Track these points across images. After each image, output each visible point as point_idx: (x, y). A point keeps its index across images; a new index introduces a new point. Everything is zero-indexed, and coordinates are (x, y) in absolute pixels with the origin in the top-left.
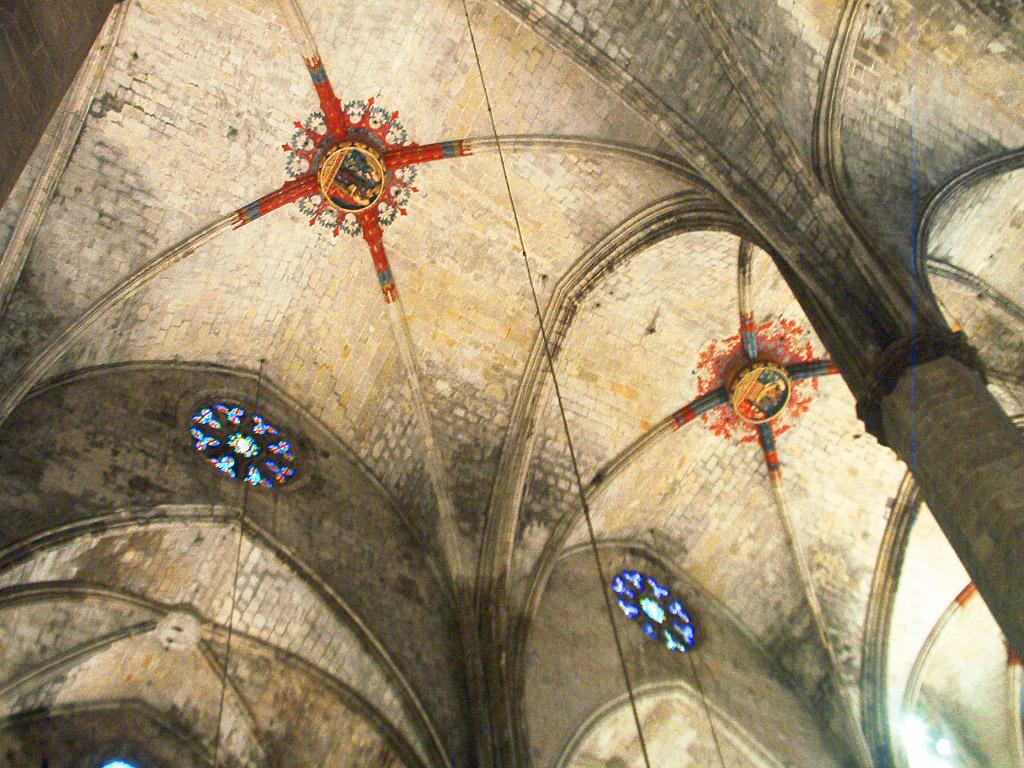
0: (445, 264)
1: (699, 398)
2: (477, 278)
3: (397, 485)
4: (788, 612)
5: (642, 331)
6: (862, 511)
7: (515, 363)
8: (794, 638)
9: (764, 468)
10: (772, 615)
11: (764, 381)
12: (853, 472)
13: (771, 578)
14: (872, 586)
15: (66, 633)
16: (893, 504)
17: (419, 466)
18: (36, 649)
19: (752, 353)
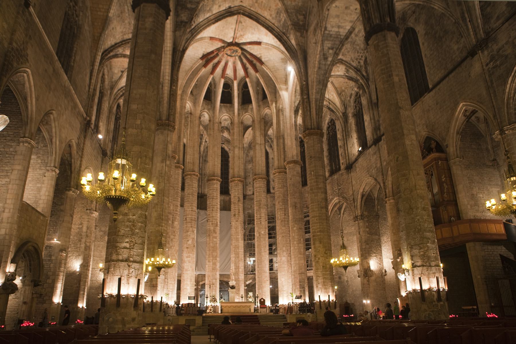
14: (209, 17)
16: (230, 7)
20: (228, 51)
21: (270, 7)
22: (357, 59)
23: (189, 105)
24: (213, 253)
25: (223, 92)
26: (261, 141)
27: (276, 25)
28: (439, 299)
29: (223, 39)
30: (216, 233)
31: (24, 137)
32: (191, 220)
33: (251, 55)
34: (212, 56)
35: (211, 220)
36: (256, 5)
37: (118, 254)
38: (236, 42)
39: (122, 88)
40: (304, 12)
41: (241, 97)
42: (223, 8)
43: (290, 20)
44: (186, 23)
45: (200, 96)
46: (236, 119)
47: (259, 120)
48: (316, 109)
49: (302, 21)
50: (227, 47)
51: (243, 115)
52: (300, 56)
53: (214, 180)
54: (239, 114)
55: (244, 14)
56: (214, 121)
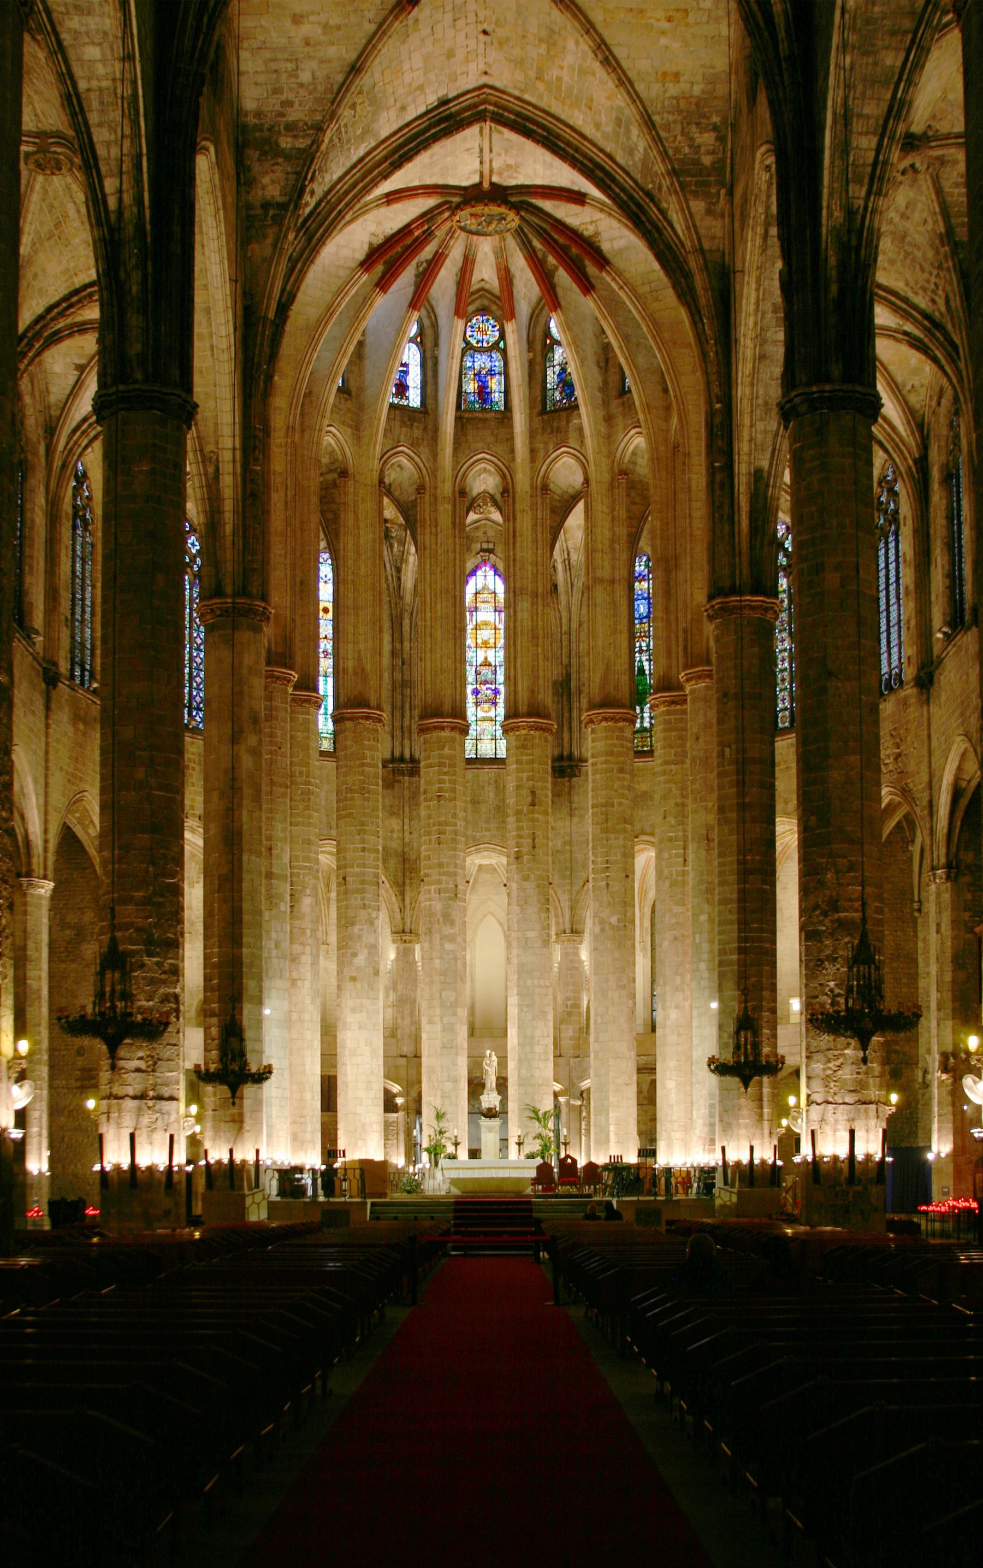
4: (291, 118)
6: (421, 88)
8: (278, 145)
10: (273, 104)
12: (450, 54)
13: (305, 77)
16: (444, 102)
20: (464, 216)
21: (592, 100)
24: (444, 993)
27: (618, 159)
29: (441, 182)
30: (452, 923)
32: (363, 882)
33: (560, 225)
34: (409, 241)
35: (435, 877)
36: (541, 86)
40: (716, 119)
43: (664, 155)
47: (607, 477)
49: (713, 153)
50: (459, 207)
52: (704, 298)
53: (443, 728)
54: (533, 451)
55: (499, 120)
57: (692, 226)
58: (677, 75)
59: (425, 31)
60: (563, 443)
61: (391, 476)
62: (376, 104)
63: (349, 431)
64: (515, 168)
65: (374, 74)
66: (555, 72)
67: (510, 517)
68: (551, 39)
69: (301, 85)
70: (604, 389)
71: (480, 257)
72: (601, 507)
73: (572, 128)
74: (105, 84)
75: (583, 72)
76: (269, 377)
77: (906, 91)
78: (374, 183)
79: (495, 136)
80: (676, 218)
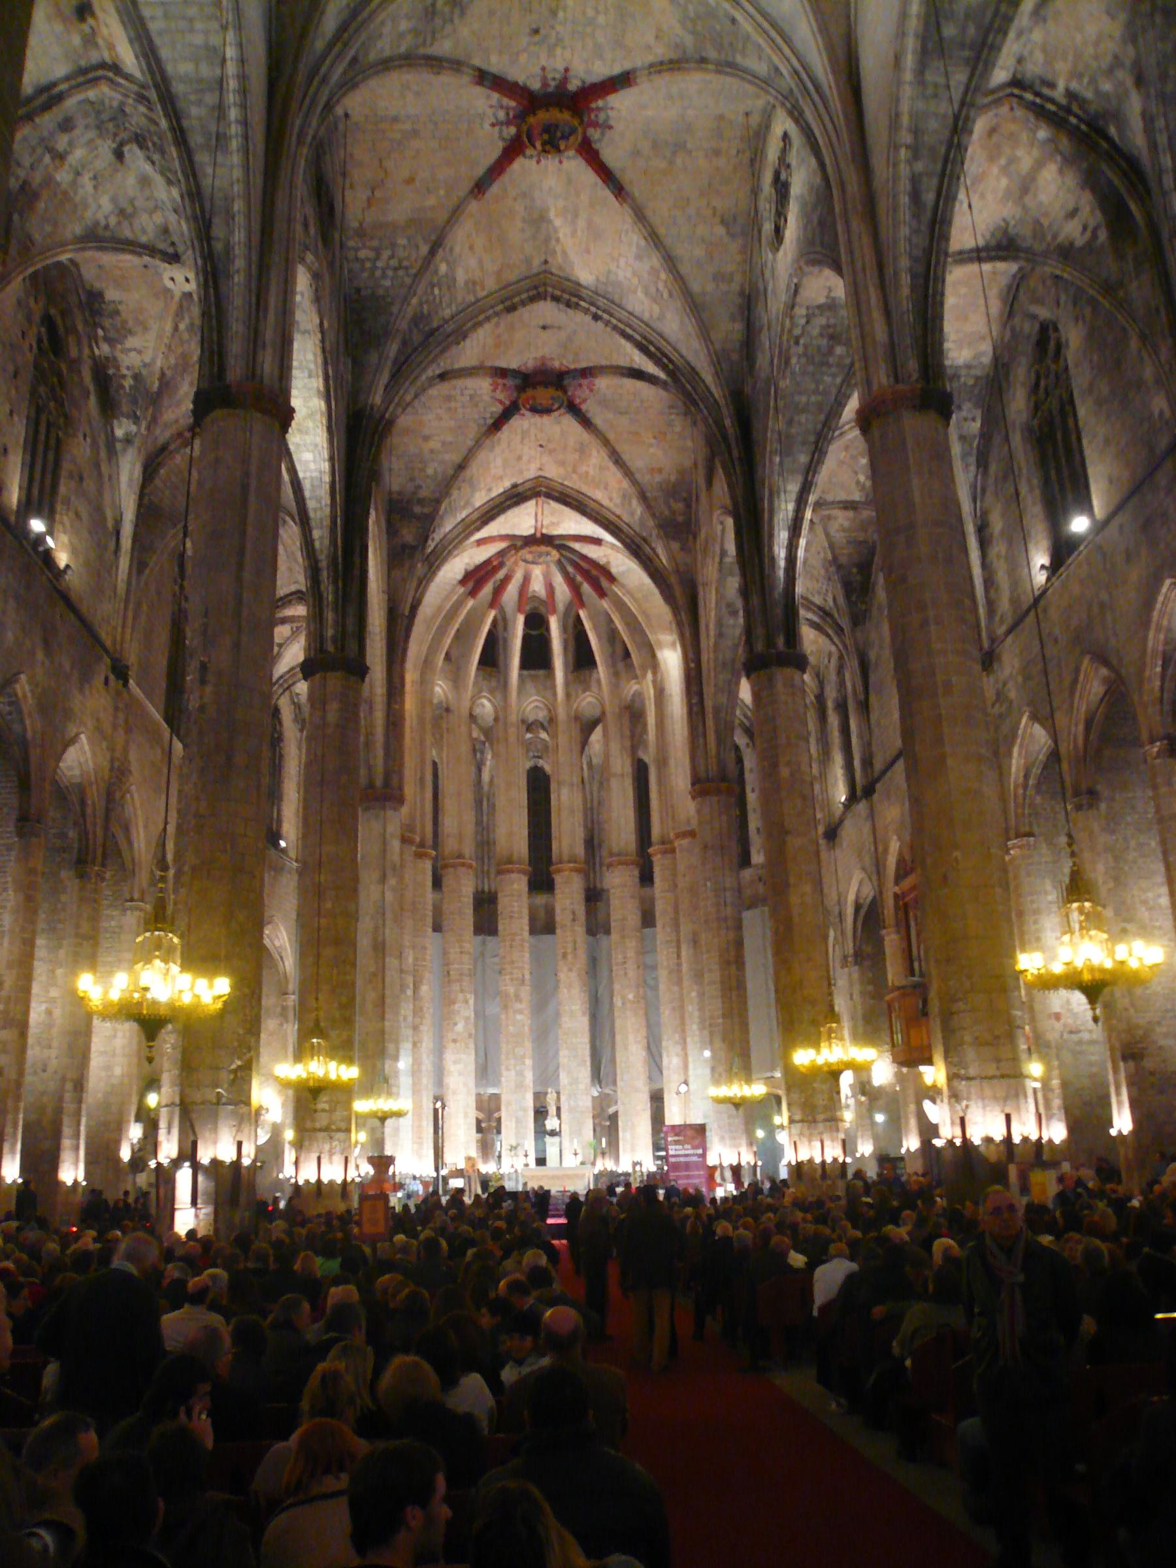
0: (519, 207)
1: (514, 371)
2: (523, 230)
3: (358, 290)
5: (541, 324)
7: (483, 289)
9: (490, 422)
10: (410, 487)
11: (553, 398)
12: (519, 458)
13: (430, 471)
15: (125, 224)
16: (515, 486)
17: (389, 300)
18: (103, 222)
19: (566, 382)
20: (525, 553)
22: (819, 593)
23: (441, 689)
25: (526, 639)
26: (623, 767)
28: (824, 1175)
29: (510, 533)
31: (132, 900)
32: (461, 974)
33: (584, 557)
36: (575, 476)
37: (313, 1121)
38: (543, 535)
39: (281, 677)
40: (684, 495)
41: (571, 648)
42: (498, 489)
43: (654, 515)
44: (414, 548)
45: (468, 662)
46: (562, 713)
47: (617, 710)
48: (717, 732)
50: (522, 547)
51: (577, 696)
54: (568, 695)
55: (549, 496)
56: (506, 718)
57: (672, 558)
58: (660, 471)
59: (504, 445)
60: (587, 689)
61: (477, 711)
62: (474, 488)
63: (450, 683)
64: (557, 524)
65: (473, 469)
66: (584, 468)
67: (554, 736)
68: (582, 450)
69: (428, 476)
70: (613, 655)
71: (533, 576)
72: (613, 730)
73: (594, 501)
74: (315, 474)
75: (601, 468)
76: (405, 651)
77: (814, 476)
78: (471, 534)
79: (545, 506)
80: (660, 551)
